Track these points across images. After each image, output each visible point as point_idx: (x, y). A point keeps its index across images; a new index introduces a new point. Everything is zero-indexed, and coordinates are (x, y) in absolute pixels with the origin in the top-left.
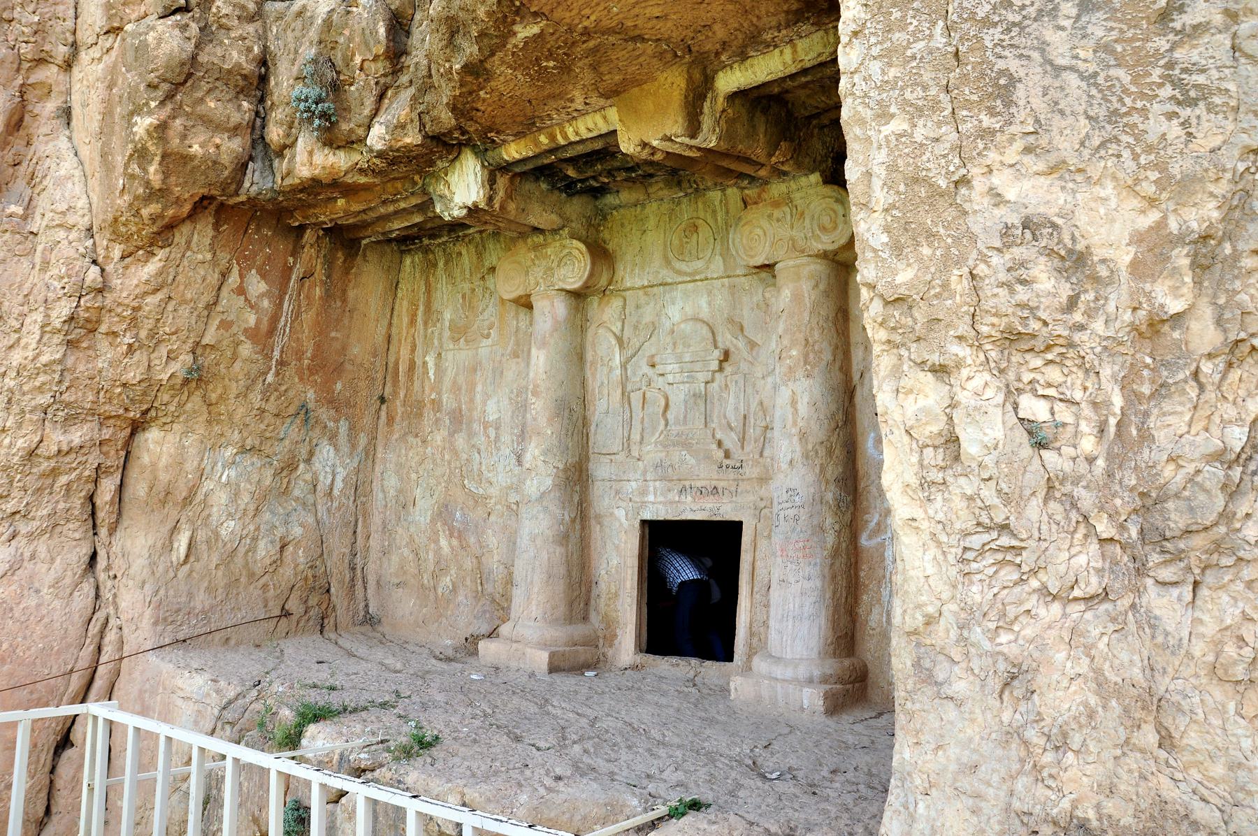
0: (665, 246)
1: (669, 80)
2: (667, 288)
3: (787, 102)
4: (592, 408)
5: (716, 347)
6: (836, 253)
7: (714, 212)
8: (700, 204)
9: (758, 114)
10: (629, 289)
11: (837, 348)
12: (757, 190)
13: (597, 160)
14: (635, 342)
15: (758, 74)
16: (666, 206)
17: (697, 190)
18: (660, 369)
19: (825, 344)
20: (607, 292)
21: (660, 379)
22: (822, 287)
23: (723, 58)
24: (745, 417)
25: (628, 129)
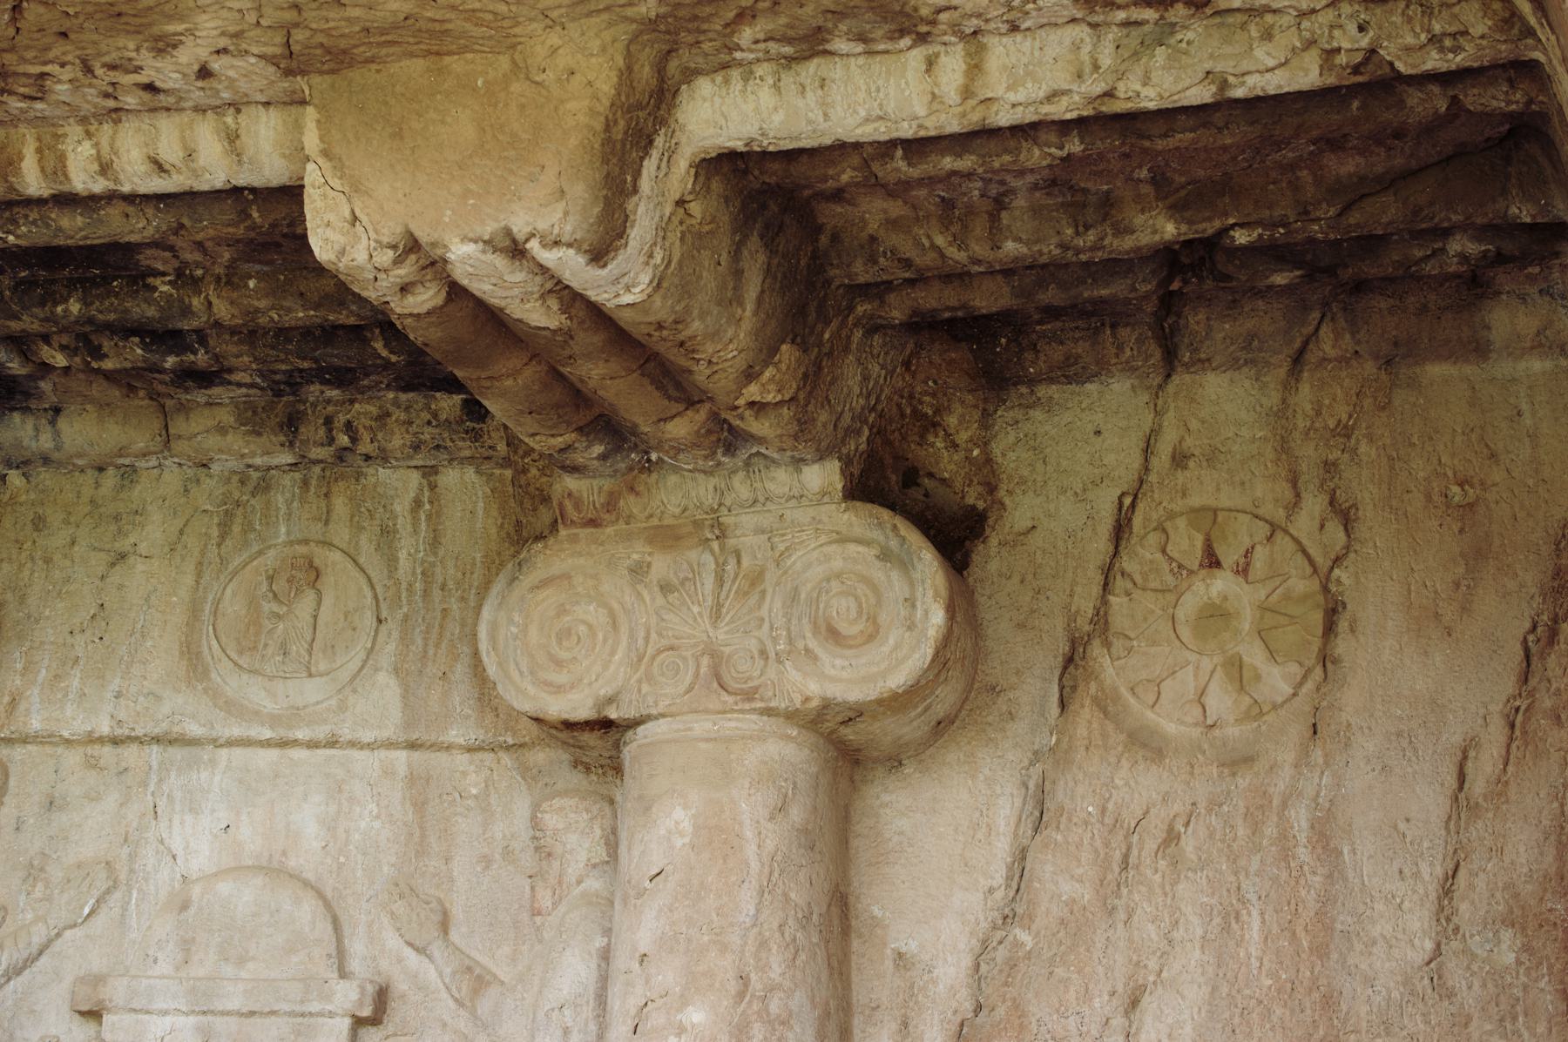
0: (195, 611)
1: (564, 59)
2: (176, 753)
3: (819, 229)
5: (343, 974)
6: (855, 714)
7: (387, 533)
8: (340, 504)
9: (754, 241)
10: (25, 740)
11: (827, 1014)
12: (607, 484)
13: (72, 284)
15: (838, 112)
16: (210, 489)
17: (341, 455)
19: (799, 999)
22: (797, 814)
23: (746, 35)
25: (356, 188)
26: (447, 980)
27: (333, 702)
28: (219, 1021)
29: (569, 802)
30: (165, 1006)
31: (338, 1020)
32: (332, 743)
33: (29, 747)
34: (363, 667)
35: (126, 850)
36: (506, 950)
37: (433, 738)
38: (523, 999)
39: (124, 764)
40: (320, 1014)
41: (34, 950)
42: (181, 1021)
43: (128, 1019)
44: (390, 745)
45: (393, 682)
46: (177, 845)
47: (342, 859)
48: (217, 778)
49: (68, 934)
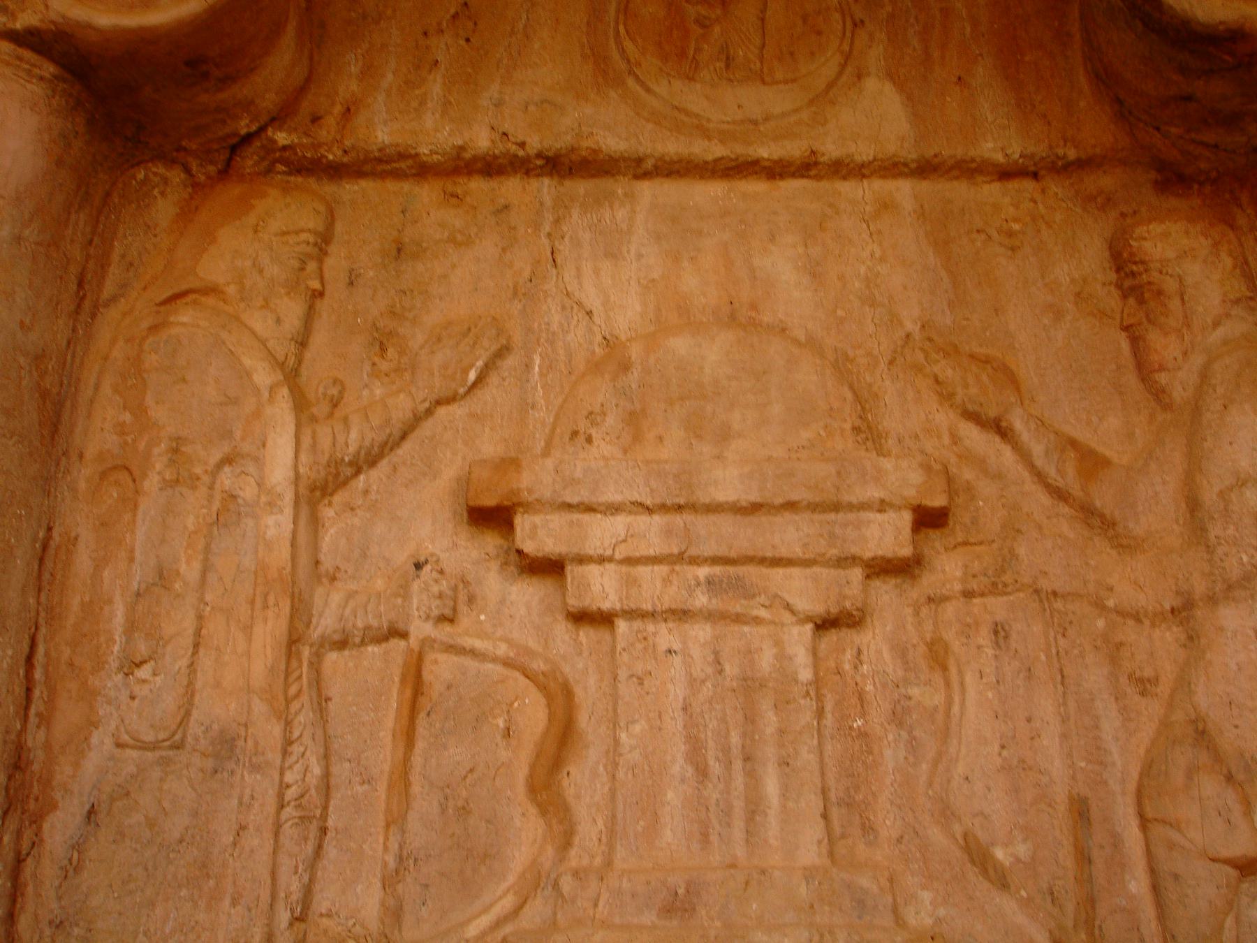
2: (581, 187)
4: (68, 714)
14: (377, 401)
18: (538, 533)
20: (249, 161)
21: (527, 595)
24: (1081, 811)
26: (1039, 463)
27: (805, 115)
28: (701, 524)
29: (1175, 228)
30: (617, 498)
31: (891, 515)
32: (807, 168)
33: (364, 183)
34: (840, 74)
35: (516, 307)
36: (1113, 422)
37: (959, 153)
38: (1164, 483)
39: (502, 201)
40: (863, 506)
41: (397, 433)
42: (643, 521)
43: (557, 521)
44: (891, 168)
45: (888, 87)
46: (592, 299)
47: (840, 313)
48: (640, 218)
49: (442, 411)
